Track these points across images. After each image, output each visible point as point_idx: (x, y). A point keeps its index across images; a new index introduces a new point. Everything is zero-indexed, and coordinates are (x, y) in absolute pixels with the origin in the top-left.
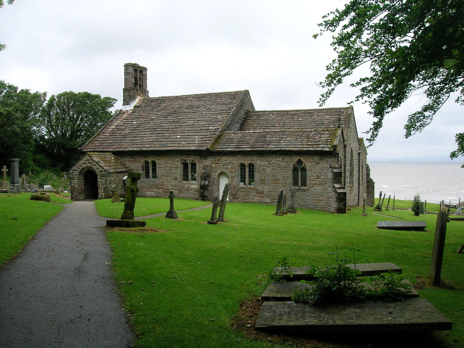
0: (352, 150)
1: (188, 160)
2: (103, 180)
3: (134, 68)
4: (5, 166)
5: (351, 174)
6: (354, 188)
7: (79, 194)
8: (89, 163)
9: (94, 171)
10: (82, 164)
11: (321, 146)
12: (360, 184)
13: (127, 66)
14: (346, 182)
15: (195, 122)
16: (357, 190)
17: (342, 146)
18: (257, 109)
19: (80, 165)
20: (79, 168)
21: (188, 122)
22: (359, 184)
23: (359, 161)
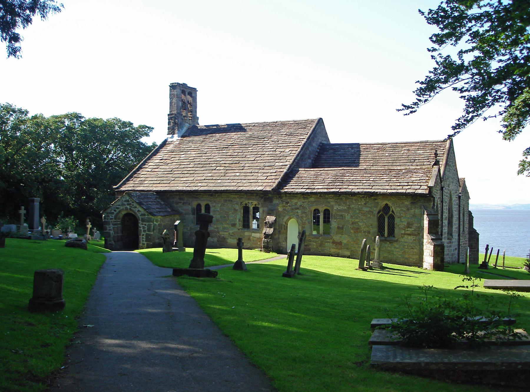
0: (450, 192)
1: (249, 203)
2: (145, 225)
3: (182, 89)
4: (23, 207)
5: (450, 223)
6: (453, 240)
7: (115, 241)
8: (128, 204)
9: (133, 213)
10: (119, 205)
11: (413, 187)
12: (461, 235)
13: (173, 87)
14: (443, 233)
15: (257, 156)
16: (457, 243)
17: (439, 188)
18: (333, 141)
19: (117, 207)
20: (115, 211)
21: (249, 156)
22: (459, 235)
23: (459, 206)
